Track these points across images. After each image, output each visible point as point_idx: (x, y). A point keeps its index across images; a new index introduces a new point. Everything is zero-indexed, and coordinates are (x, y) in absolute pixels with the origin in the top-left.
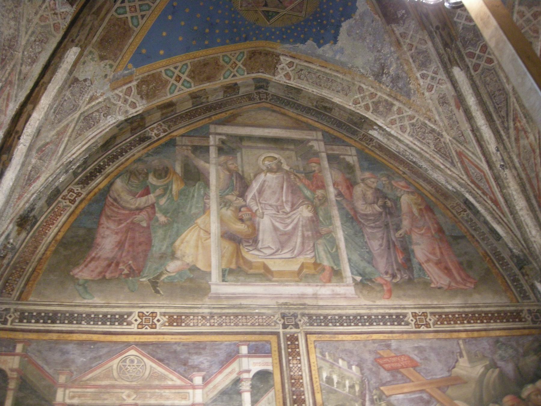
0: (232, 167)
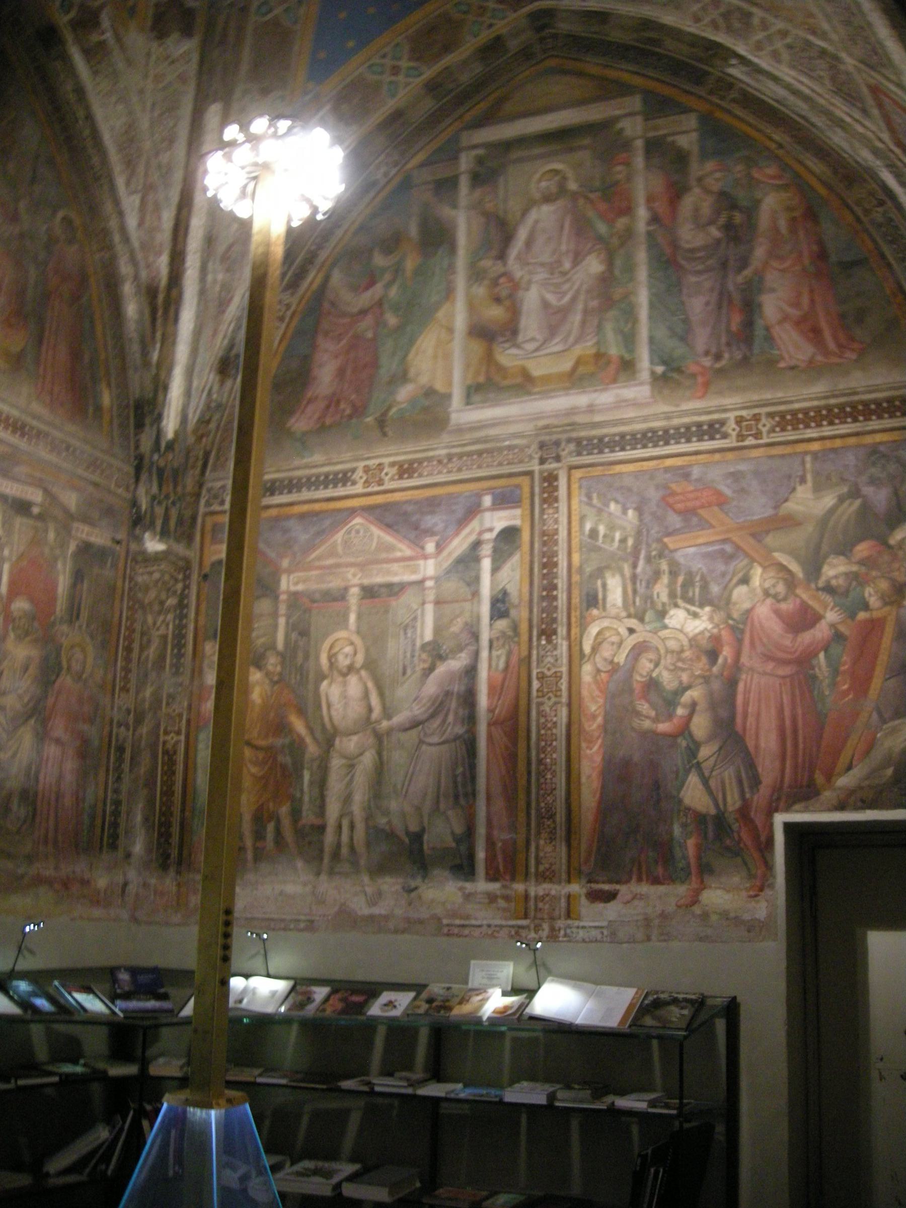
0: (489, 206)
